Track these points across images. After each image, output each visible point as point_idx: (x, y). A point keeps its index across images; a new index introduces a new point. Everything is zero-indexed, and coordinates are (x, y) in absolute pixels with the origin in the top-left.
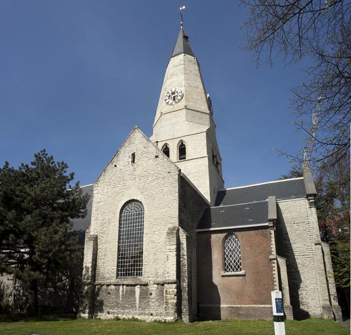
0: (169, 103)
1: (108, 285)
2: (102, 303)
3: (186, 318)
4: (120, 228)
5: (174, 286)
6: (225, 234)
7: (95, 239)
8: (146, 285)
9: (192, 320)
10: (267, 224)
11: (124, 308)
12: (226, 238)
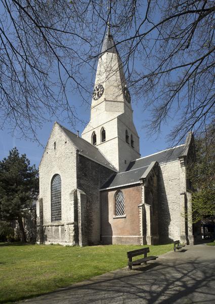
0: (96, 98)
1: (48, 226)
2: (46, 236)
3: (81, 244)
4: (51, 192)
5: (73, 225)
6: (115, 191)
7: (41, 200)
8: (63, 225)
9: (84, 245)
10: (139, 182)
11: (55, 238)
12: (117, 194)
